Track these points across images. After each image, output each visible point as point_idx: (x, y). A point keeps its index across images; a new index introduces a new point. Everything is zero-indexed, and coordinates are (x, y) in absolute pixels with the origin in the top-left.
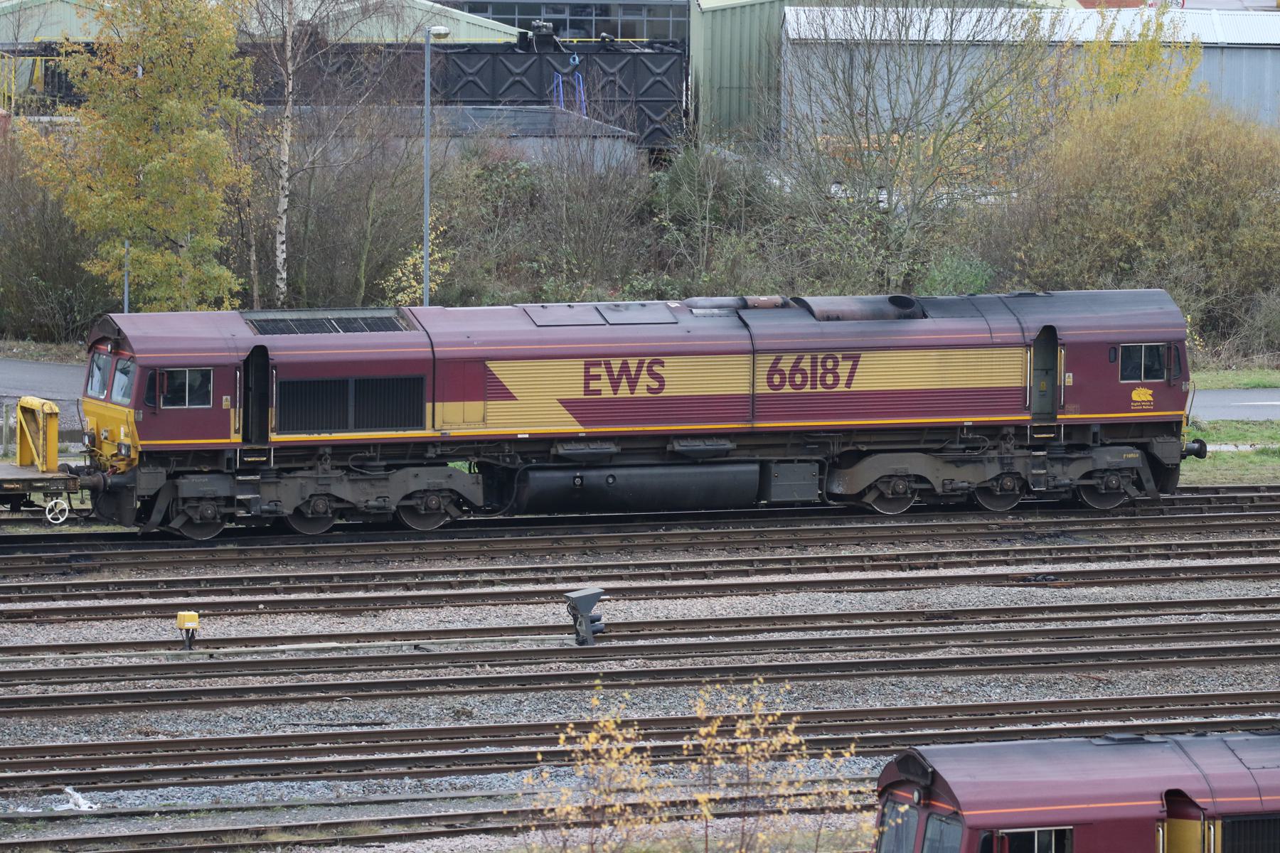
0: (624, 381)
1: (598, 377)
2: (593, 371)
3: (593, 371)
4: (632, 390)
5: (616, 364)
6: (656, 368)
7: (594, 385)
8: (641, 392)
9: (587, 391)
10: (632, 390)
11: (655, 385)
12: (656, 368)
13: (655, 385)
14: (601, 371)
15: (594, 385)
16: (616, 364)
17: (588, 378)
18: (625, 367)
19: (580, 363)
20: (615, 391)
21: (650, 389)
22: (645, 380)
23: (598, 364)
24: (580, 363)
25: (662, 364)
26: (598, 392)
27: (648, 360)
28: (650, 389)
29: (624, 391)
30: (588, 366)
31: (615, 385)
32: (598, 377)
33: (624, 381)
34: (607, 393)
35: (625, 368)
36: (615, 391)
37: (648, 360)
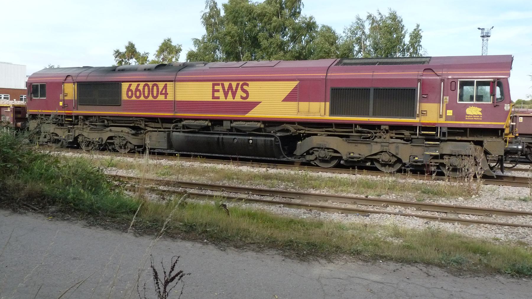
0: (230, 93)
1: (218, 91)
2: (216, 88)
3: (216, 88)
4: (234, 97)
6: (245, 87)
7: (216, 94)
8: (238, 99)
9: (214, 97)
10: (234, 98)
11: (244, 95)
12: (245, 87)
13: (244, 95)
14: (219, 88)
15: (216, 94)
16: (226, 84)
17: (214, 91)
18: (230, 86)
20: (226, 98)
21: (242, 97)
22: (240, 93)
23: (218, 85)
24: (211, 84)
25: (247, 85)
26: (218, 98)
27: (241, 83)
28: (242, 97)
29: (230, 98)
30: (214, 85)
31: (226, 95)
32: (218, 91)
33: (230, 93)
34: (222, 99)
35: (230, 86)
36: (226, 98)
37: (241, 83)
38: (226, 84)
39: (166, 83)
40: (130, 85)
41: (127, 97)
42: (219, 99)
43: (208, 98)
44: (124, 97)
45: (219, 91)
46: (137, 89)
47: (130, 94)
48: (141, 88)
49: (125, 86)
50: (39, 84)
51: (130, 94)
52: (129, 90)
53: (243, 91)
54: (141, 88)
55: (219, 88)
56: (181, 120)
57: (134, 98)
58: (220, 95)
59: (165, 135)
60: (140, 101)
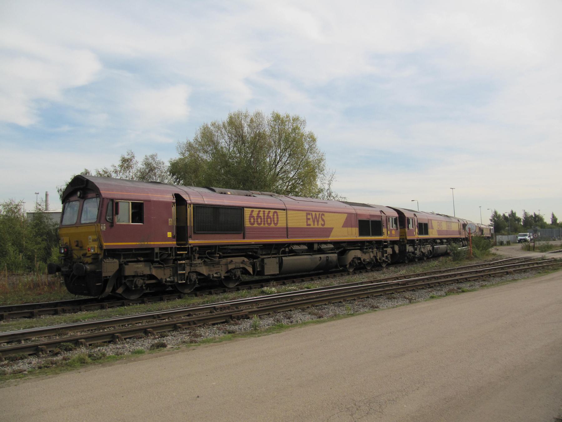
1: (309, 219)
3: (309, 217)
5: (314, 213)
7: (309, 222)
8: (320, 226)
9: (308, 225)
15: (309, 222)
17: (308, 219)
19: (305, 213)
22: (321, 222)
24: (305, 213)
25: (323, 215)
26: (310, 225)
29: (316, 226)
30: (307, 214)
32: (309, 219)
34: (312, 226)
38: (314, 213)
39: (270, 210)
40: (252, 211)
41: (249, 224)
42: (310, 226)
43: (305, 226)
44: (247, 224)
45: (310, 220)
46: (258, 216)
47: (252, 221)
48: (261, 214)
49: (247, 212)
50: (130, 201)
51: (252, 221)
52: (251, 216)
53: (322, 220)
54: (271, 215)
55: (309, 217)
56: (289, 244)
57: (256, 225)
58: (310, 222)
59: (277, 260)
60: (262, 228)
